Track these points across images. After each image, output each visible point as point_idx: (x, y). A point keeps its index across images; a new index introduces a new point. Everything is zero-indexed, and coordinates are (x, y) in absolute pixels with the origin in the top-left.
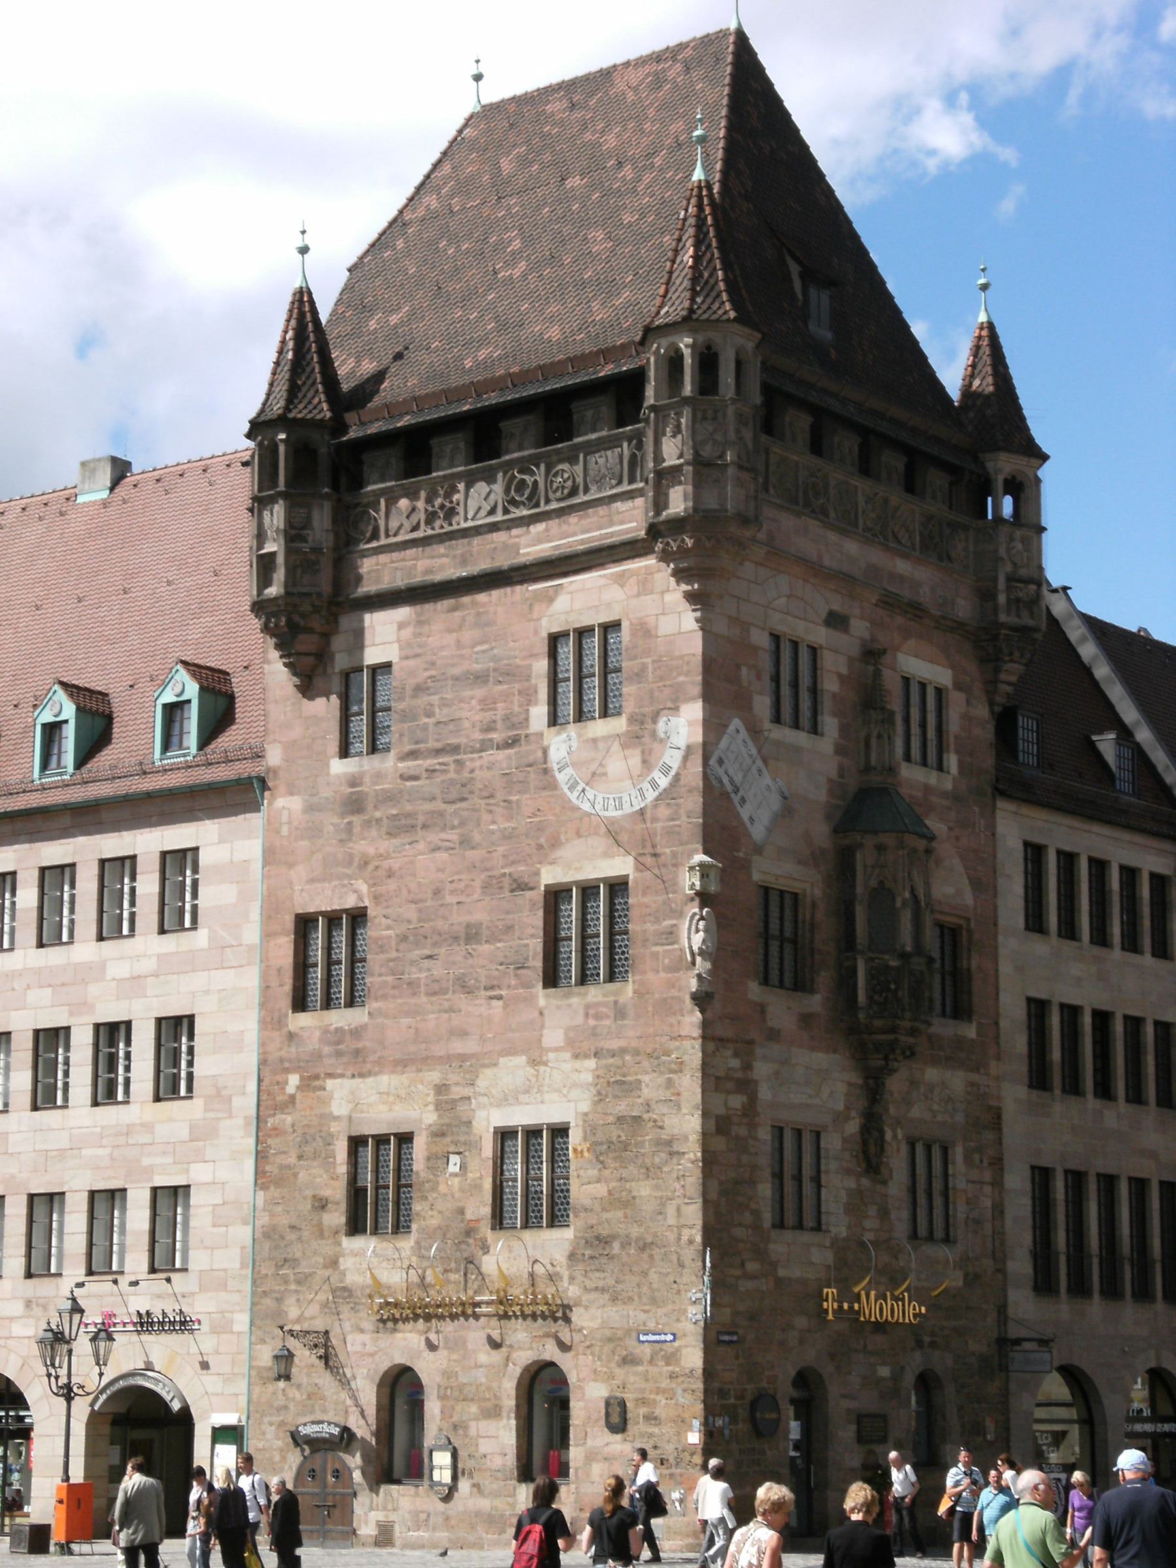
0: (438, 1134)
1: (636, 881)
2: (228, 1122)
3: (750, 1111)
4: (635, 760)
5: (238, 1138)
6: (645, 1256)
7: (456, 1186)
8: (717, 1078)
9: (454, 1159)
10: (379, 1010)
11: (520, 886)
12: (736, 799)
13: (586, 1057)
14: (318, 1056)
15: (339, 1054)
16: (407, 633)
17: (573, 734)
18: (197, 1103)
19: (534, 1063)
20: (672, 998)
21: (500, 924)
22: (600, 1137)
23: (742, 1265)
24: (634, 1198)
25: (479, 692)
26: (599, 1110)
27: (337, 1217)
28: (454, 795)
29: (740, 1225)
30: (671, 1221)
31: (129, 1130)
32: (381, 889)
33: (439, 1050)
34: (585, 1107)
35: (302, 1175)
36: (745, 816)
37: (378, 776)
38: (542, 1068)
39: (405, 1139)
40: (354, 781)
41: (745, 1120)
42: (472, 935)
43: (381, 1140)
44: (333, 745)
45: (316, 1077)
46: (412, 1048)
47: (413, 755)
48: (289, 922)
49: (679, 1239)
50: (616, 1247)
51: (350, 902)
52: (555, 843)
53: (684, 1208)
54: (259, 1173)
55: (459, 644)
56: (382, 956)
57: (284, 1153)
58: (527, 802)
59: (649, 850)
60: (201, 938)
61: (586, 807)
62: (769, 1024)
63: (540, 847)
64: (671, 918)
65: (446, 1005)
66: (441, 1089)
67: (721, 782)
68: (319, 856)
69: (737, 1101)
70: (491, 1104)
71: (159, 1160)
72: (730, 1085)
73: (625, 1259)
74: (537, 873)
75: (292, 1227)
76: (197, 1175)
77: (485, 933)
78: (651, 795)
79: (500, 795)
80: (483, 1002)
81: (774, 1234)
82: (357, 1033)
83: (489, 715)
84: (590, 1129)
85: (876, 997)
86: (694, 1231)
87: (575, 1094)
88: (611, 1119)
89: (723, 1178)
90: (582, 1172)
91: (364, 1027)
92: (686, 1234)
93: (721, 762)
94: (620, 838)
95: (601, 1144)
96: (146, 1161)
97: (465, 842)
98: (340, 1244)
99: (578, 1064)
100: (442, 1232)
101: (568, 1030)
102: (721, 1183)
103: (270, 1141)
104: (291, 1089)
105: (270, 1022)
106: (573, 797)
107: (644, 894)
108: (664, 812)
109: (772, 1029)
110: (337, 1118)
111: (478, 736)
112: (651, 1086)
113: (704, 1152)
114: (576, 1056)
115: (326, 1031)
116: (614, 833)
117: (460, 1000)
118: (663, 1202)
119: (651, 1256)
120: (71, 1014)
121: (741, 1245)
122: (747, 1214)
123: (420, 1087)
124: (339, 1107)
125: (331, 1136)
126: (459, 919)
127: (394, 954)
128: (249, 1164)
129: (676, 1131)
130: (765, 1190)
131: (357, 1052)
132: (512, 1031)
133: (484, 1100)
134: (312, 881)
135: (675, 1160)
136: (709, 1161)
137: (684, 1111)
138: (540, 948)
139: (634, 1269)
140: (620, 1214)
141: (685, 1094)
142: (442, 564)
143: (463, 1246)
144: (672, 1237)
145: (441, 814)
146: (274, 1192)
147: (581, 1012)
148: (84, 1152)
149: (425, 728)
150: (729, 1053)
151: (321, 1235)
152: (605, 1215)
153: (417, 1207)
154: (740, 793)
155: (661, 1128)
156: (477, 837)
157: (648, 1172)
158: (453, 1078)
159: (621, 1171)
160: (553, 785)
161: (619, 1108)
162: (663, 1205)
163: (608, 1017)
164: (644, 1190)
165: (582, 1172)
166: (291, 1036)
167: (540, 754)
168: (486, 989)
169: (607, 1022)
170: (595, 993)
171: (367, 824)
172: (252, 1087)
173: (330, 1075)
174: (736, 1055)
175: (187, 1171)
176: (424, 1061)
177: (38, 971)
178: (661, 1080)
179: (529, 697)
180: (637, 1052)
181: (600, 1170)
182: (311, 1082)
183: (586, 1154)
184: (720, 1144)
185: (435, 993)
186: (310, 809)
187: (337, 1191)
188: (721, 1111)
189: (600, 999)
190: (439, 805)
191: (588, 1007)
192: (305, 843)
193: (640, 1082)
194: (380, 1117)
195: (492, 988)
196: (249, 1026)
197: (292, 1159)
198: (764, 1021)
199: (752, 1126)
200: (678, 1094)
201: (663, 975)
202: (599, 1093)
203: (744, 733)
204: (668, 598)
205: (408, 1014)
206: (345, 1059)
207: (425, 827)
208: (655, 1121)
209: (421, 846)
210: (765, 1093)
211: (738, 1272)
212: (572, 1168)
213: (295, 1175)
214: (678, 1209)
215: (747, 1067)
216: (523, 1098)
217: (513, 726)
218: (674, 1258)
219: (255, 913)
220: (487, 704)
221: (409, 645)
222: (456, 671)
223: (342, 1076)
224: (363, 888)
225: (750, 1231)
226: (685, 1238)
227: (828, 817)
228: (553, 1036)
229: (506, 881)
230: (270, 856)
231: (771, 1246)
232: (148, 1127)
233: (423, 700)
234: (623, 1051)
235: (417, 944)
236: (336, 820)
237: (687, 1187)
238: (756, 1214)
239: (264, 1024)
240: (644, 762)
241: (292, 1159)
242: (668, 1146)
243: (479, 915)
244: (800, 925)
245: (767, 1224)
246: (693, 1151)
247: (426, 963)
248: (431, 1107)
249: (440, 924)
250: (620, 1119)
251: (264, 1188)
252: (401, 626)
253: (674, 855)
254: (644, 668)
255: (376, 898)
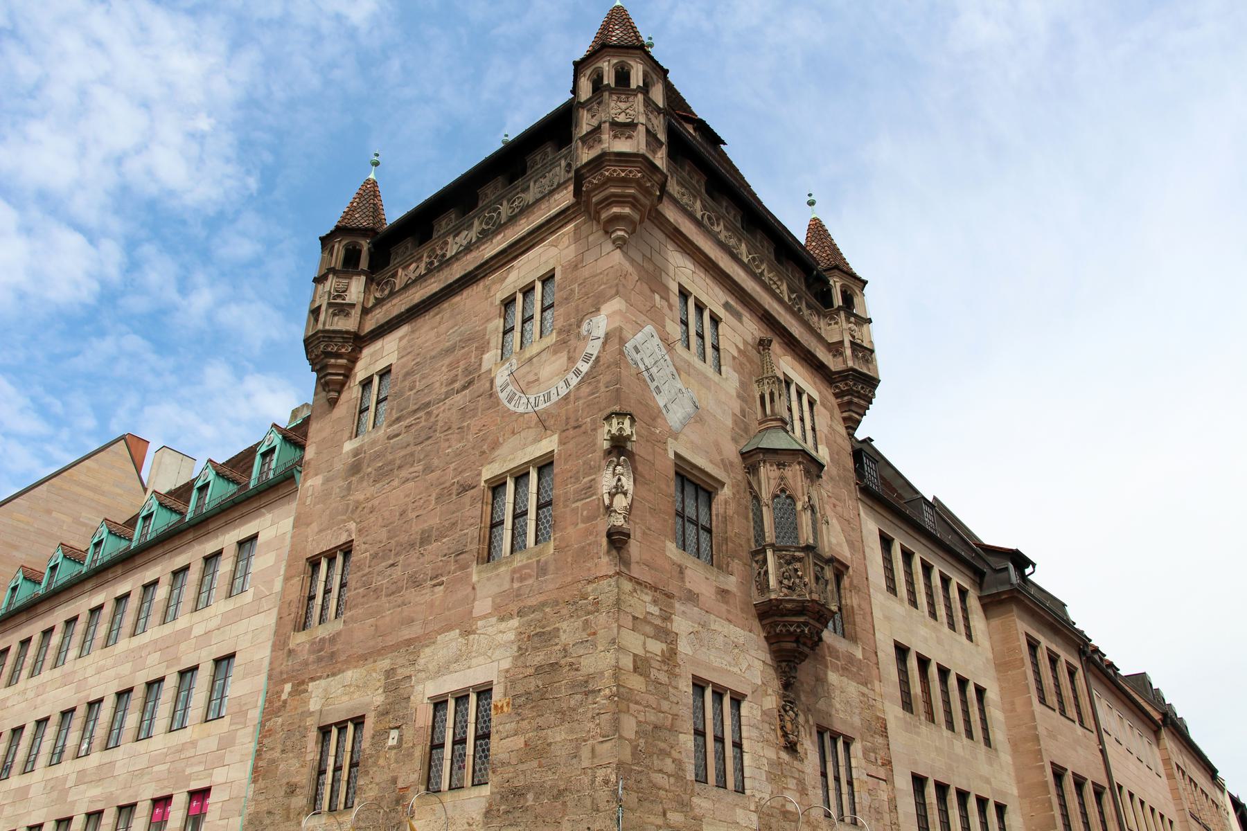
0: (383, 713)
1: (560, 455)
2: (243, 731)
3: (670, 657)
4: (562, 359)
5: (247, 742)
6: (558, 804)
7: (394, 761)
8: (635, 618)
9: (394, 734)
10: (352, 617)
11: (465, 488)
12: (653, 386)
13: (511, 617)
14: (306, 664)
15: (320, 660)
16: (405, 341)
17: (514, 361)
18: (227, 719)
19: (467, 633)
20: (589, 544)
21: (446, 523)
22: (520, 689)
23: (664, 814)
24: (549, 745)
25: (447, 361)
26: (519, 664)
27: (300, 801)
28: (423, 436)
29: (660, 771)
30: (586, 764)
31: (182, 748)
32: (364, 524)
33: (390, 641)
34: (506, 664)
35: (282, 767)
36: (661, 404)
37: (374, 443)
38: (471, 637)
39: (359, 722)
40: (356, 452)
41: (665, 668)
42: (425, 539)
43: (342, 727)
44: (347, 434)
45: (303, 682)
46: (371, 643)
47: (398, 420)
48: (302, 563)
49: (593, 782)
50: (530, 796)
51: (343, 539)
52: (495, 445)
53: (599, 748)
54: (255, 769)
55: (438, 335)
56: (360, 574)
57: (273, 749)
58: (474, 424)
59: (572, 423)
60: (248, 596)
61: (521, 409)
62: (688, 585)
63: (484, 452)
64: (590, 475)
65: (400, 601)
66: (389, 673)
67: (636, 363)
68: (328, 512)
69: (656, 647)
70: (427, 678)
71: (195, 769)
72: (648, 629)
73: (539, 810)
74: (479, 474)
75: (269, 813)
76: (218, 777)
77: (434, 533)
78: (574, 381)
79: (455, 426)
80: (427, 591)
81: (698, 787)
82: (333, 639)
83: (454, 373)
84: (511, 681)
85: (786, 582)
86: (609, 770)
87: (498, 654)
88: (531, 671)
89: (641, 718)
90: (500, 728)
91: (339, 634)
92: (601, 773)
93: (637, 350)
94: (547, 424)
95: (520, 696)
96: (188, 771)
97: (428, 469)
98: (299, 824)
99: (503, 626)
100: (378, 802)
101: (494, 598)
102: (639, 723)
103: (265, 741)
104: (284, 696)
105: (280, 643)
106: (511, 407)
107: (566, 461)
108: (585, 390)
109: (690, 591)
110: (311, 714)
111: (444, 390)
112: (569, 631)
113: (618, 686)
114: (502, 619)
115: (313, 643)
116: (543, 423)
117: (411, 594)
118: (578, 743)
119: (564, 803)
120: (167, 667)
121: (662, 793)
122: (669, 761)
123: (374, 675)
124: (314, 705)
125: (306, 729)
126: (417, 528)
127: (367, 570)
128: (249, 764)
129: (592, 670)
130: (687, 741)
131: (333, 655)
132: (449, 609)
133: (423, 675)
134: (321, 531)
135: (590, 699)
136: (622, 698)
137: (600, 648)
138: (476, 534)
139: (547, 820)
140: (535, 764)
141: (601, 632)
142: (434, 286)
143: (393, 814)
144: (586, 780)
145: (412, 454)
146: (261, 783)
147: (508, 578)
148: (156, 769)
149: (408, 399)
150: (648, 598)
151: (288, 818)
152: (521, 767)
153: (361, 782)
154: (655, 383)
155: (577, 670)
156: (436, 462)
157: (565, 715)
158: (400, 661)
159: (538, 719)
160: (498, 402)
161: (538, 659)
162: (578, 748)
163: (530, 576)
164: (559, 735)
165: (500, 728)
166: (290, 651)
167: (488, 385)
168: (431, 579)
169: (530, 581)
170: (520, 559)
171: (362, 479)
172: (261, 702)
173: (312, 679)
174: (655, 602)
175: (211, 775)
176: (379, 653)
177: (155, 642)
178: (579, 623)
179: (483, 349)
180: (557, 603)
181: (518, 722)
182: (299, 689)
183: (505, 709)
184: (636, 683)
185: (393, 593)
186: (327, 480)
187: (304, 777)
188: (640, 652)
189: (525, 562)
190: (408, 450)
191: (514, 571)
192: (320, 506)
193: (558, 629)
194: (342, 708)
195: (437, 577)
196: (264, 654)
197: (276, 754)
198: (682, 579)
199: (672, 675)
200: (594, 634)
201: (581, 526)
202: (520, 648)
203: (656, 340)
204: (591, 238)
205: (371, 615)
206: (323, 664)
207: (400, 467)
208: (571, 664)
209: (396, 483)
210: (684, 647)
211: (660, 821)
212: (493, 724)
213: (277, 767)
214: (593, 750)
215: (667, 618)
216: (454, 666)
217: (470, 373)
218: (588, 802)
219: (282, 572)
220: (451, 367)
221: (405, 348)
222: (433, 353)
223: (320, 678)
224: (352, 526)
225: (672, 780)
226: (599, 779)
227: (734, 440)
228: (483, 606)
229: (455, 487)
230: (296, 525)
231: (695, 800)
232: (193, 744)
233: (407, 383)
234: (544, 604)
235: (384, 558)
236: (341, 483)
237: (602, 725)
238: (679, 763)
239: (275, 648)
240: (569, 358)
241: (276, 754)
242: (586, 688)
243: (435, 521)
244: (714, 518)
245: (691, 776)
246: (606, 685)
247: (389, 571)
248: (381, 691)
249: (403, 538)
250: (539, 670)
251: (255, 781)
252: (401, 339)
253: (594, 421)
254: (572, 291)
255: (360, 531)
